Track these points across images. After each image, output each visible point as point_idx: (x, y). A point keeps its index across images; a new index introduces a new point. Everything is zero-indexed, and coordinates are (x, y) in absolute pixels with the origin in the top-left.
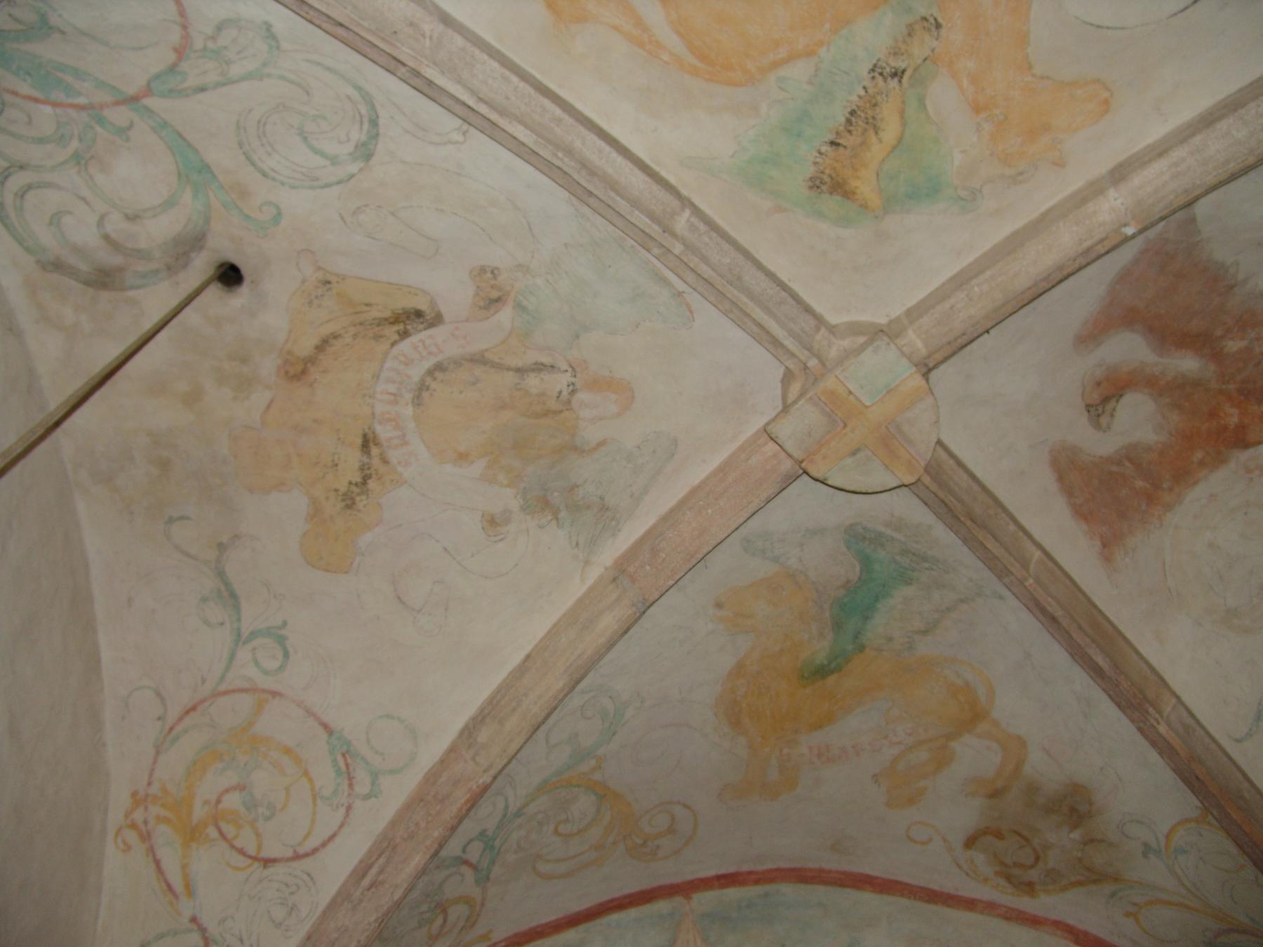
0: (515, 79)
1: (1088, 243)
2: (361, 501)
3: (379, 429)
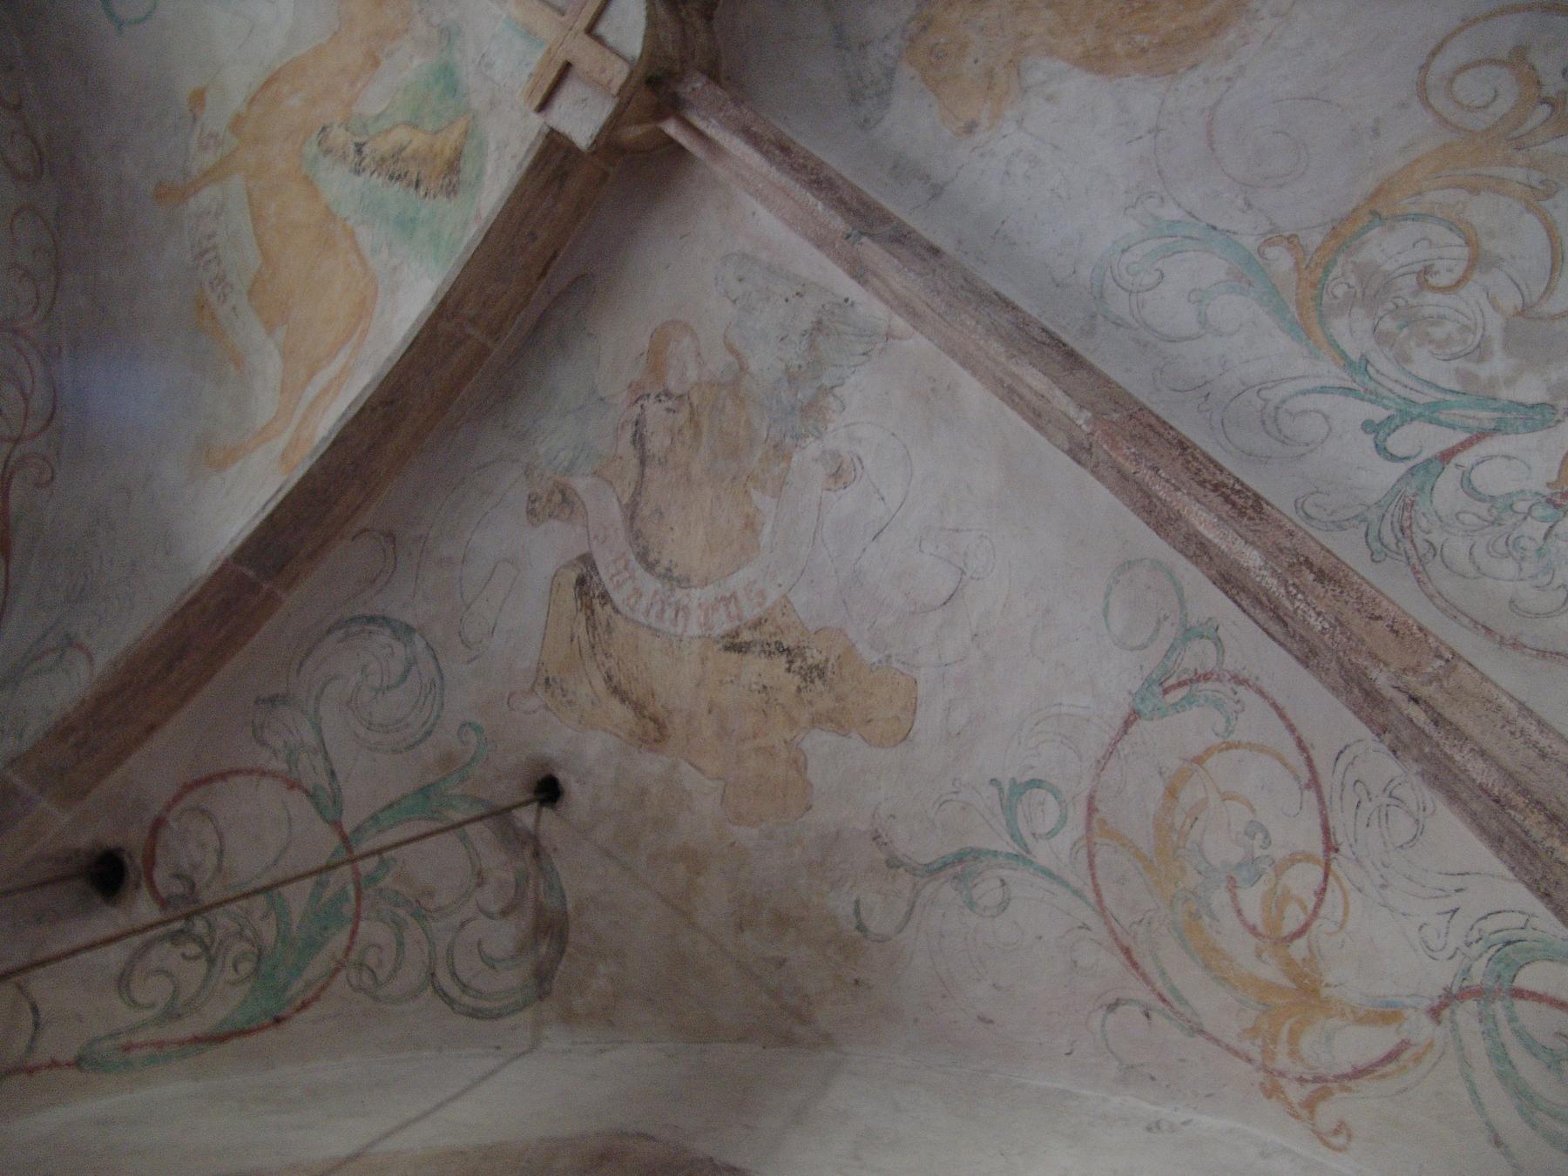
2: (814, 656)
3: (718, 631)
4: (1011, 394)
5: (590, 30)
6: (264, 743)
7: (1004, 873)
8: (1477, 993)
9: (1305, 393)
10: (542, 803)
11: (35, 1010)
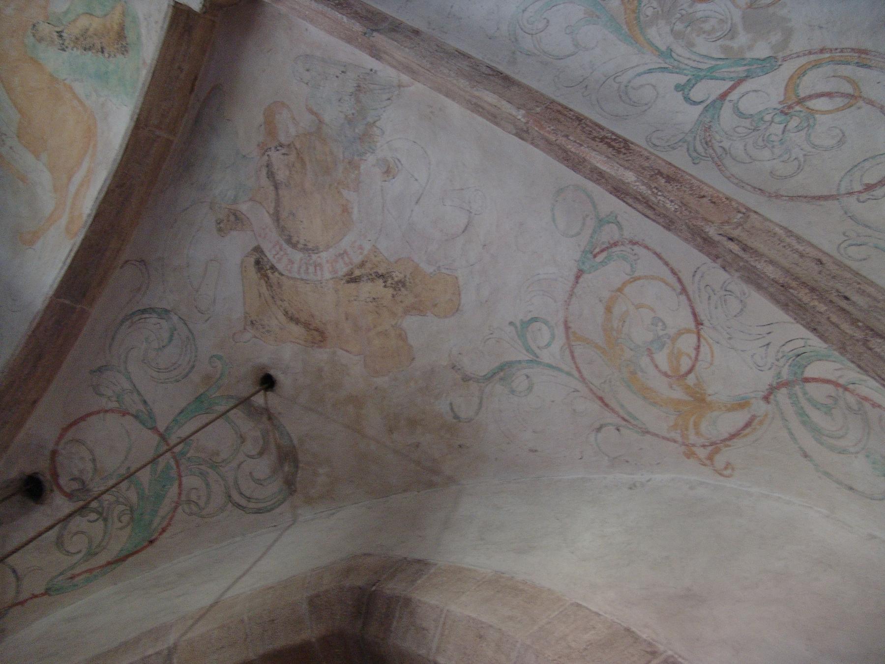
2: (398, 276)
3: (341, 273)
4: (477, 107)
6: (102, 395)
7: (526, 371)
8: (786, 384)
9: (639, 75)
10: (266, 390)
11: (14, 571)
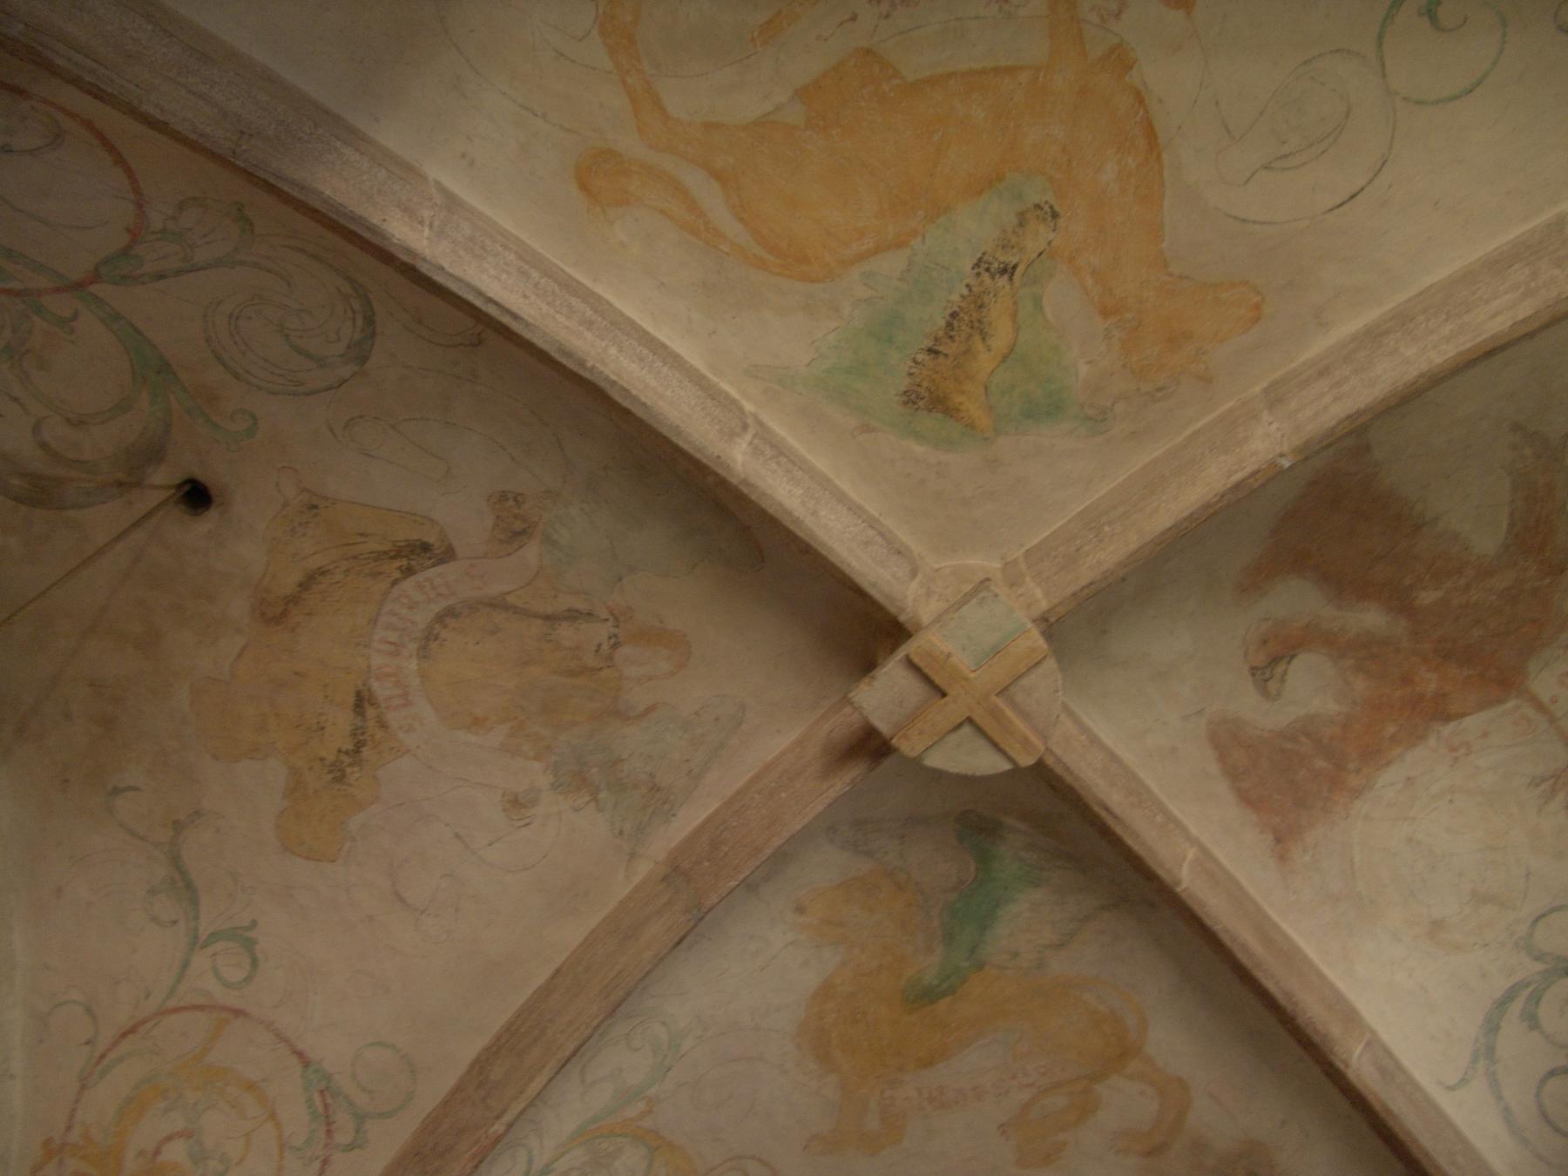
0: (535, 274)
1: (1237, 477)
3: (375, 685)
5: (970, 720)
6: (181, 207)
